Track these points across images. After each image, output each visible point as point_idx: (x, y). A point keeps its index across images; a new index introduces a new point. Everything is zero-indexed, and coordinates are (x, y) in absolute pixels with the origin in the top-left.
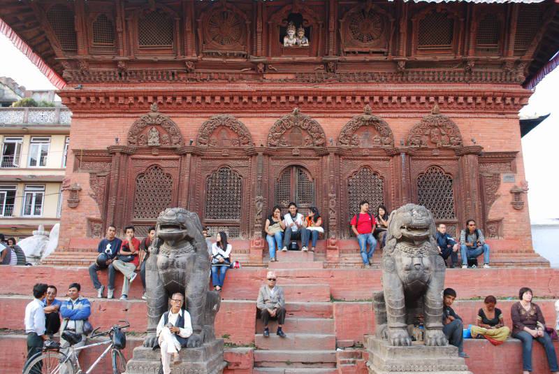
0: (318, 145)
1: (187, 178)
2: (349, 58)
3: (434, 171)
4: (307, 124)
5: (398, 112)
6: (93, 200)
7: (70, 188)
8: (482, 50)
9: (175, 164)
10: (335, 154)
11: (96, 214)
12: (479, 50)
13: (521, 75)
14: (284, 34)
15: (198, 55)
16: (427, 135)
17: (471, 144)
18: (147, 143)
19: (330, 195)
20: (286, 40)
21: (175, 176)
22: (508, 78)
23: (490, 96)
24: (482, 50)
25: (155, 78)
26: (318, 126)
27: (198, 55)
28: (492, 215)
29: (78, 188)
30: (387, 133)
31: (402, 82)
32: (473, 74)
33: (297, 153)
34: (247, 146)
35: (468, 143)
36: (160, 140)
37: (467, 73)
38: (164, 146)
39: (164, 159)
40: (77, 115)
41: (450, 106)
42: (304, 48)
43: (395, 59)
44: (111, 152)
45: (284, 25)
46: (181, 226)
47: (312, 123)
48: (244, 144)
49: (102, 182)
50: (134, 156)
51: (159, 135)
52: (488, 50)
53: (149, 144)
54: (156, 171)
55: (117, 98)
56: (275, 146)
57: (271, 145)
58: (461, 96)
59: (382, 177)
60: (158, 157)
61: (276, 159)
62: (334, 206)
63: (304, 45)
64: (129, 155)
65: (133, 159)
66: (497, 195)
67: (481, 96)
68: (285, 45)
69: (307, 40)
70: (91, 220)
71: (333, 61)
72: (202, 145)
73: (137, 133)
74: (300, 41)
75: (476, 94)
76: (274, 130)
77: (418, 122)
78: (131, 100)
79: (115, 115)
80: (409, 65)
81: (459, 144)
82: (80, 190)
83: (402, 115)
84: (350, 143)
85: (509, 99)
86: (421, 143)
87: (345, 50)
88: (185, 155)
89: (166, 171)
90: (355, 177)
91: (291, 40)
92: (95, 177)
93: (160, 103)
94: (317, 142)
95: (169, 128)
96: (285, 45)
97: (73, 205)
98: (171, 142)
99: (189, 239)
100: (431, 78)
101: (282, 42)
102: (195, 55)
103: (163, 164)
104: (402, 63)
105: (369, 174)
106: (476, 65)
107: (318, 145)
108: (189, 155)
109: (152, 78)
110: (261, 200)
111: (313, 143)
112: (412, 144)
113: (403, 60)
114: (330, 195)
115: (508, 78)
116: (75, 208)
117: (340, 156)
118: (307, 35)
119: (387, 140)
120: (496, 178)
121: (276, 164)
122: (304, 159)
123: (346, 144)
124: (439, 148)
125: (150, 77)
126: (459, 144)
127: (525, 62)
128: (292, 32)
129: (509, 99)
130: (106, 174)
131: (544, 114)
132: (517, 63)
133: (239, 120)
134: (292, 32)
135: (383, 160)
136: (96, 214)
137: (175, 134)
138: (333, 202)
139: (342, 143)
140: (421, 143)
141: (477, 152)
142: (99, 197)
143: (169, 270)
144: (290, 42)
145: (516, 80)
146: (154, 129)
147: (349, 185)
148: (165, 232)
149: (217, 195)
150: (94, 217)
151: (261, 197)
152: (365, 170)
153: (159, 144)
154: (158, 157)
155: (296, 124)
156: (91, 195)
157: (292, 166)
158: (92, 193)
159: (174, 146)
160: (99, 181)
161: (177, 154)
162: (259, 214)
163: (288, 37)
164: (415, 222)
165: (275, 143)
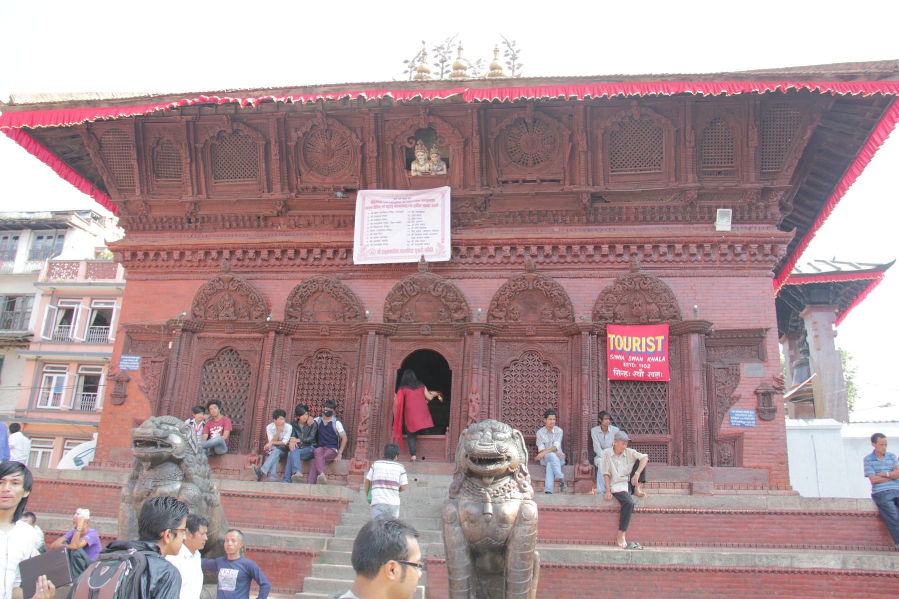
2: (509, 190)
4: (440, 289)
5: (583, 269)
8: (711, 173)
10: (482, 334)
12: (705, 173)
13: (776, 210)
14: (410, 159)
15: (291, 190)
16: (623, 304)
17: (692, 317)
20: (414, 166)
22: (754, 215)
23: (724, 242)
24: (711, 173)
25: (234, 224)
26: (456, 292)
27: (291, 190)
28: (724, 429)
29: (125, 378)
30: (561, 302)
31: (589, 222)
32: (698, 209)
33: (427, 332)
34: (356, 322)
35: (687, 315)
37: (689, 209)
38: (241, 320)
39: (240, 339)
40: (137, 277)
41: (663, 259)
42: (440, 176)
43: (574, 190)
44: (169, 328)
45: (410, 146)
46: (159, 443)
50: (201, 334)
51: (234, 305)
52: (720, 173)
53: (221, 319)
55: (182, 254)
56: (395, 321)
57: (389, 321)
58: (693, 243)
59: (555, 370)
60: (233, 336)
61: (397, 340)
63: (441, 173)
64: (194, 332)
65: (199, 338)
67: (709, 242)
68: (413, 174)
69: (445, 166)
71: (481, 195)
72: (293, 320)
73: (202, 301)
74: (435, 167)
75: (703, 239)
76: (391, 298)
77: (609, 283)
79: (182, 276)
80: (595, 197)
81: (674, 317)
82: (128, 381)
83: (588, 273)
85: (754, 246)
87: (500, 179)
88: (268, 332)
89: (242, 357)
90: (514, 368)
94: (456, 315)
96: (413, 174)
98: (250, 315)
99: (172, 460)
100: (632, 217)
101: (409, 168)
102: (287, 191)
103: (240, 347)
104: (585, 195)
105: (536, 363)
106: (700, 196)
107: (457, 321)
109: (231, 225)
111: (450, 316)
112: (601, 318)
113: (587, 192)
115: (754, 215)
117: (491, 336)
119: (560, 313)
121: (400, 348)
122: (440, 340)
125: (227, 224)
126: (674, 317)
127: (780, 189)
129: (754, 246)
131: (885, 263)
132: (765, 192)
133: (344, 282)
134: (420, 155)
135: (555, 342)
138: (474, 407)
139: (495, 318)
141: (701, 328)
142: (150, 392)
144: (423, 169)
145: (766, 217)
147: (505, 381)
149: (310, 392)
152: (531, 357)
153: (235, 318)
154: (233, 336)
155: (424, 289)
156: (141, 388)
158: (142, 384)
159: (254, 320)
160: (153, 368)
161: (260, 332)
165: (394, 317)
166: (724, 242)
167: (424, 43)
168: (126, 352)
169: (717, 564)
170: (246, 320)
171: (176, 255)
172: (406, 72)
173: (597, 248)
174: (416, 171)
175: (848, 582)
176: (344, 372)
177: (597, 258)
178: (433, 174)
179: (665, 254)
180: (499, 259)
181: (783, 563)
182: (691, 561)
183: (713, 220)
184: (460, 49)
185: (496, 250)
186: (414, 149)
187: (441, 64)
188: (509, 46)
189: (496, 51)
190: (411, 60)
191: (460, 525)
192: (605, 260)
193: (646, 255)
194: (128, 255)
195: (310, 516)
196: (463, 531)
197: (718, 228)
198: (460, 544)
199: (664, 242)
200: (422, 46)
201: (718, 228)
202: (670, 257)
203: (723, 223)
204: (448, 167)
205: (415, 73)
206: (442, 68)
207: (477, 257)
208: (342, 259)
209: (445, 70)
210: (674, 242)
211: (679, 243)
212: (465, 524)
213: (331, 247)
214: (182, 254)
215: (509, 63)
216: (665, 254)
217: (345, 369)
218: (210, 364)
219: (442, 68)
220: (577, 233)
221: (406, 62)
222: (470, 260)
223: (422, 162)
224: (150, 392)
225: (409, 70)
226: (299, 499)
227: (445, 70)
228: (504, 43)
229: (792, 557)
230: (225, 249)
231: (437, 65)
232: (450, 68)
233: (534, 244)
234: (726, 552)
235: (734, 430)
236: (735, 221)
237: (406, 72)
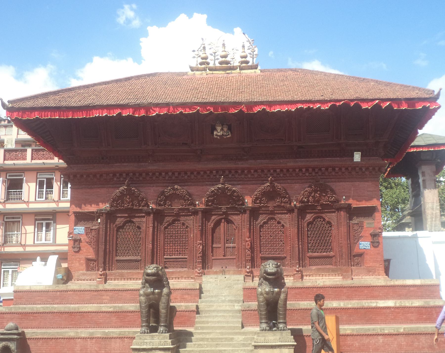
0: (239, 205)
1: (151, 230)
3: (319, 220)
6: (89, 246)
7: (73, 238)
9: (144, 219)
11: (92, 255)
14: (214, 129)
18: (124, 206)
19: (247, 239)
20: (215, 133)
21: (143, 228)
23: (357, 167)
29: (78, 238)
34: (191, 208)
36: (133, 205)
47: (234, 191)
48: (189, 205)
49: (93, 233)
54: (130, 224)
55: (101, 176)
59: (283, 226)
62: (249, 247)
66: (361, 237)
70: (88, 260)
74: (225, 133)
78: (111, 175)
84: (260, 203)
86: (308, 201)
89: (137, 225)
91: (219, 133)
92: (88, 231)
93: (131, 178)
95: (138, 196)
97: (76, 250)
101: (213, 133)
108: (152, 215)
110: (200, 244)
114: (247, 239)
116: (78, 252)
118: (230, 129)
120: (360, 225)
123: (258, 203)
124: (322, 205)
128: (219, 128)
130: (96, 227)
134: (219, 128)
136: (92, 255)
137: (142, 200)
138: (248, 244)
140: (308, 201)
142: (92, 244)
143: (151, 296)
144: (219, 134)
146: (128, 197)
148: (147, 277)
150: (90, 257)
151: (201, 242)
156: (87, 242)
157: (222, 219)
158: (87, 240)
162: (200, 253)
163: (217, 130)
164: (269, 271)
166: (357, 167)
167: (203, 39)
168: (76, 225)
169: (350, 306)
170: (137, 208)
171: (98, 176)
172: (194, 57)
173: (301, 170)
174: (216, 135)
175: (397, 310)
176: (186, 229)
177: (301, 174)
178: (225, 137)
179: (331, 172)
180: (256, 176)
181: (374, 305)
182: (340, 305)
183: (353, 156)
184: (224, 45)
185: (254, 171)
186: (215, 125)
187: (214, 54)
188: (250, 43)
189: (243, 47)
190: (196, 50)
191: (263, 295)
192: (304, 175)
193: (322, 173)
194: (71, 177)
195: (187, 296)
196: (265, 298)
197: (355, 160)
198: (263, 302)
199: (331, 167)
200: (201, 42)
201: (355, 160)
202: (333, 173)
203: (357, 157)
204: (231, 133)
205: (200, 60)
206: (215, 57)
207: (246, 175)
208: (182, 177)
209: (216, 58)
210: (335, 167)
211: (337, 167)
212: (265, 295)
213: (177, 172)
214: (101, 176)
215: (250, 54)
216: (331, 172)
217: (187, 228)
218: (119, 229)
219: (215, 57)
220: (291, 163)
221: (194, 51)
222: (243, 176)
223: (219, 131)
224: (92, 244)
225: (196, 56)
226: (181, 289)
227: (216, 58)
228: (247, 41)
229: (377, 303)
230: (124, 173)
231: (211, 55)
232: (219, 57)
233: (272, 169)
234: (354, 302)
235: (361, 251)
236: (362, 156)
237: (194, 57)
